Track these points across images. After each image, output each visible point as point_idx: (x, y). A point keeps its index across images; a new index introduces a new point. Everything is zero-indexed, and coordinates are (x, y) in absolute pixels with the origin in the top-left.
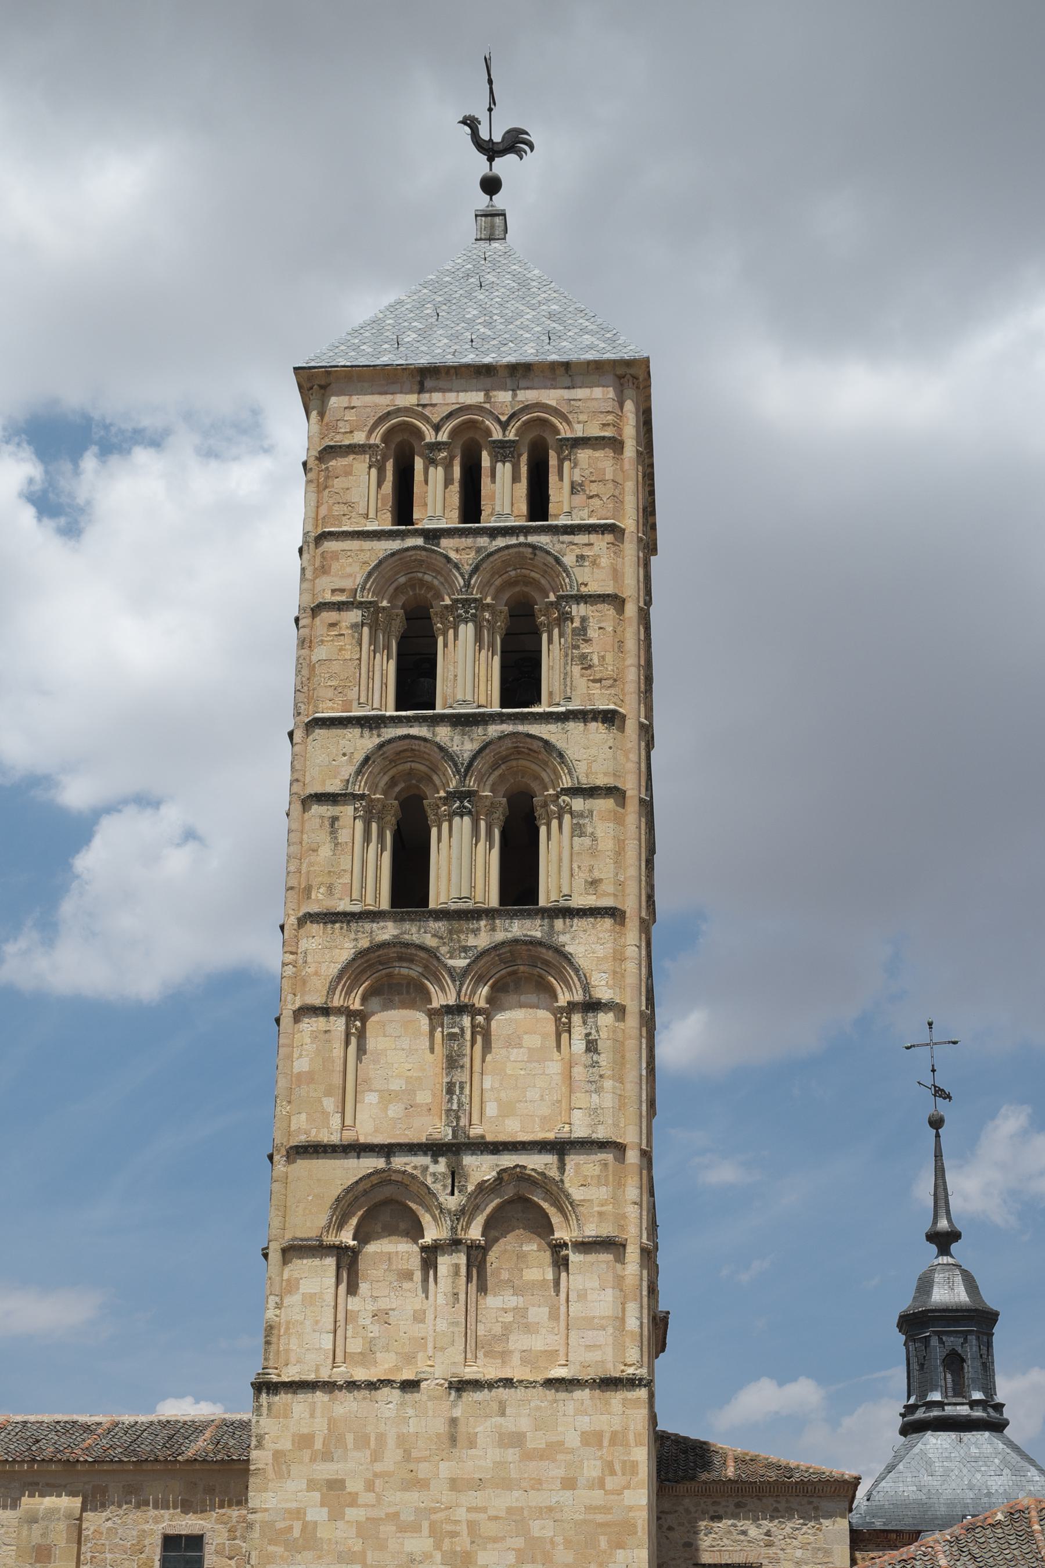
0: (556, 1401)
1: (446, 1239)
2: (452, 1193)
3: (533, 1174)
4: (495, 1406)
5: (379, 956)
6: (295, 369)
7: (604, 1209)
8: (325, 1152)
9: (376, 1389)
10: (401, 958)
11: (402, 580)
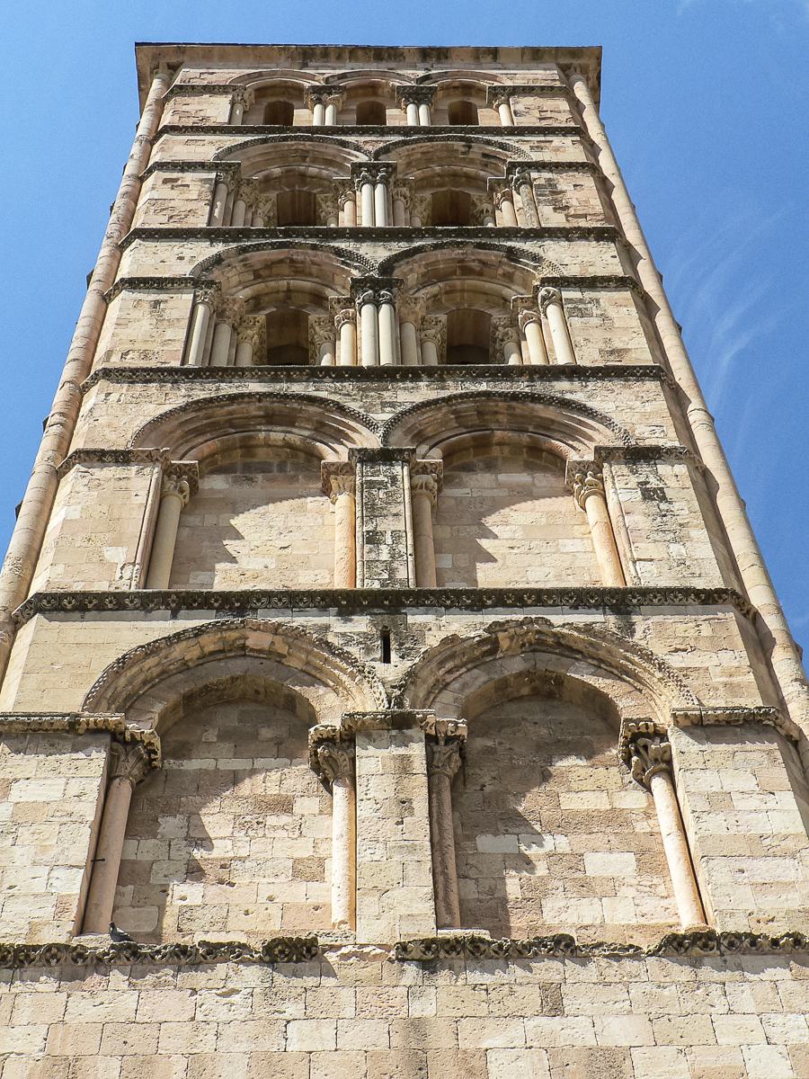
0: (699, 984)
1: (375, 714)
2: (386, 659)
3: (565, 631)
4: (533, 997)
5: (230, 413)
6: (137, 44)
7: (735, 680)
8: (100, 608)
9: (195, 966)
10: (271, 419)
11: (277, 171)
